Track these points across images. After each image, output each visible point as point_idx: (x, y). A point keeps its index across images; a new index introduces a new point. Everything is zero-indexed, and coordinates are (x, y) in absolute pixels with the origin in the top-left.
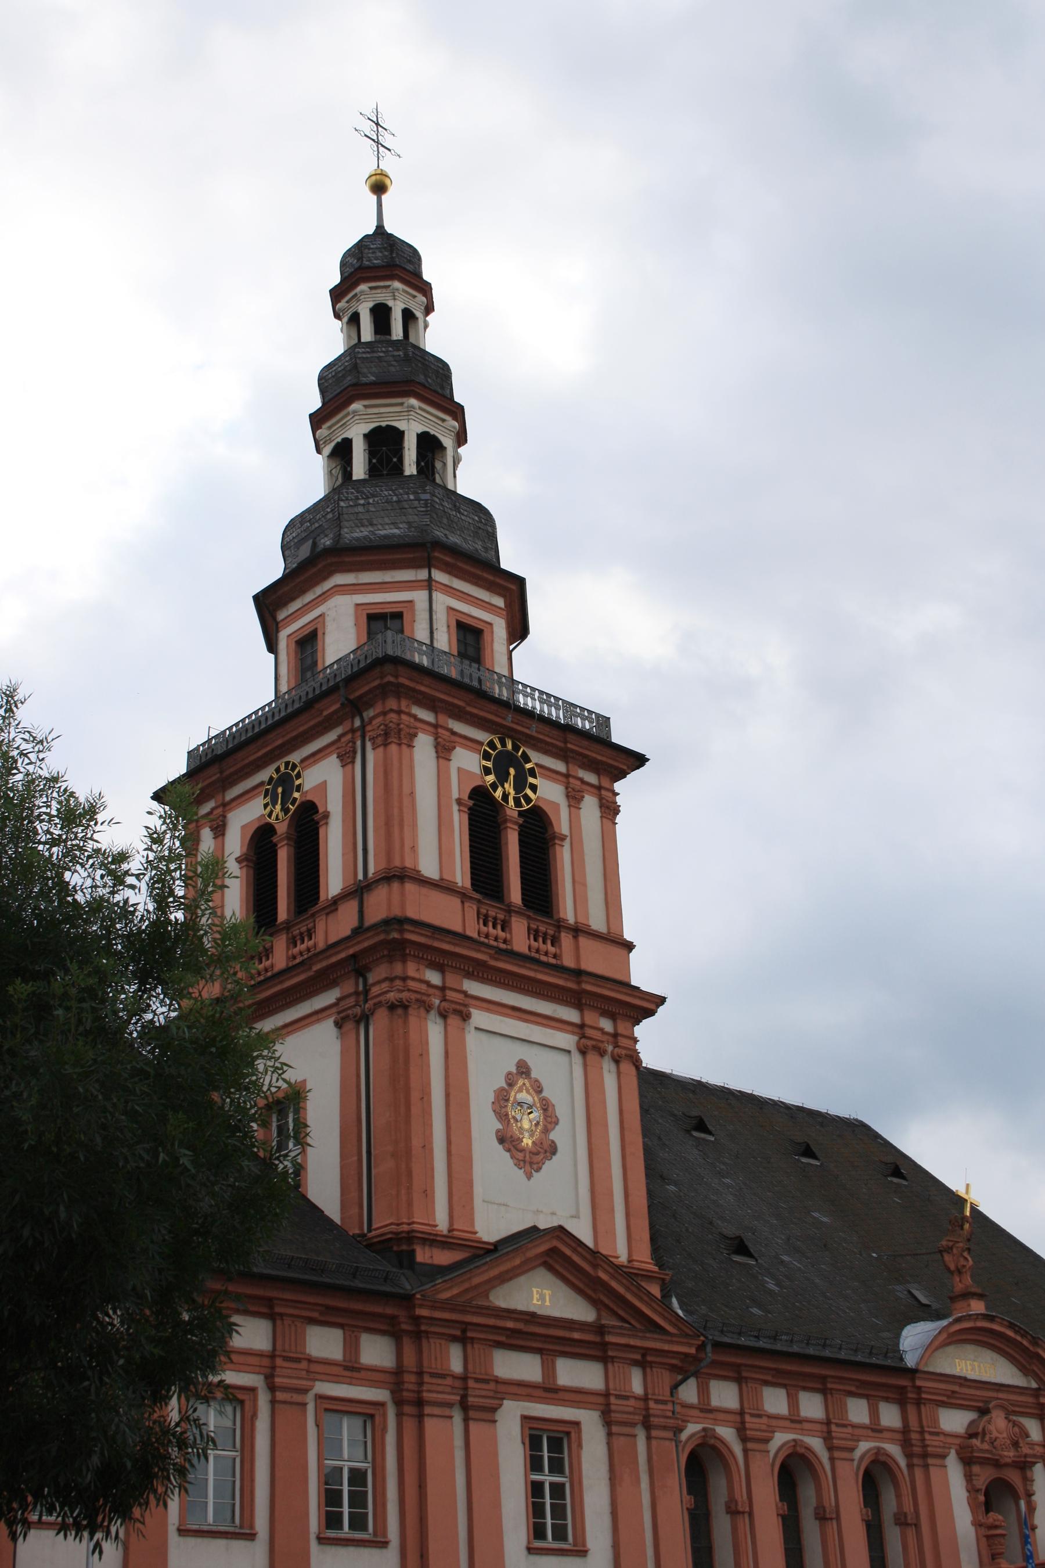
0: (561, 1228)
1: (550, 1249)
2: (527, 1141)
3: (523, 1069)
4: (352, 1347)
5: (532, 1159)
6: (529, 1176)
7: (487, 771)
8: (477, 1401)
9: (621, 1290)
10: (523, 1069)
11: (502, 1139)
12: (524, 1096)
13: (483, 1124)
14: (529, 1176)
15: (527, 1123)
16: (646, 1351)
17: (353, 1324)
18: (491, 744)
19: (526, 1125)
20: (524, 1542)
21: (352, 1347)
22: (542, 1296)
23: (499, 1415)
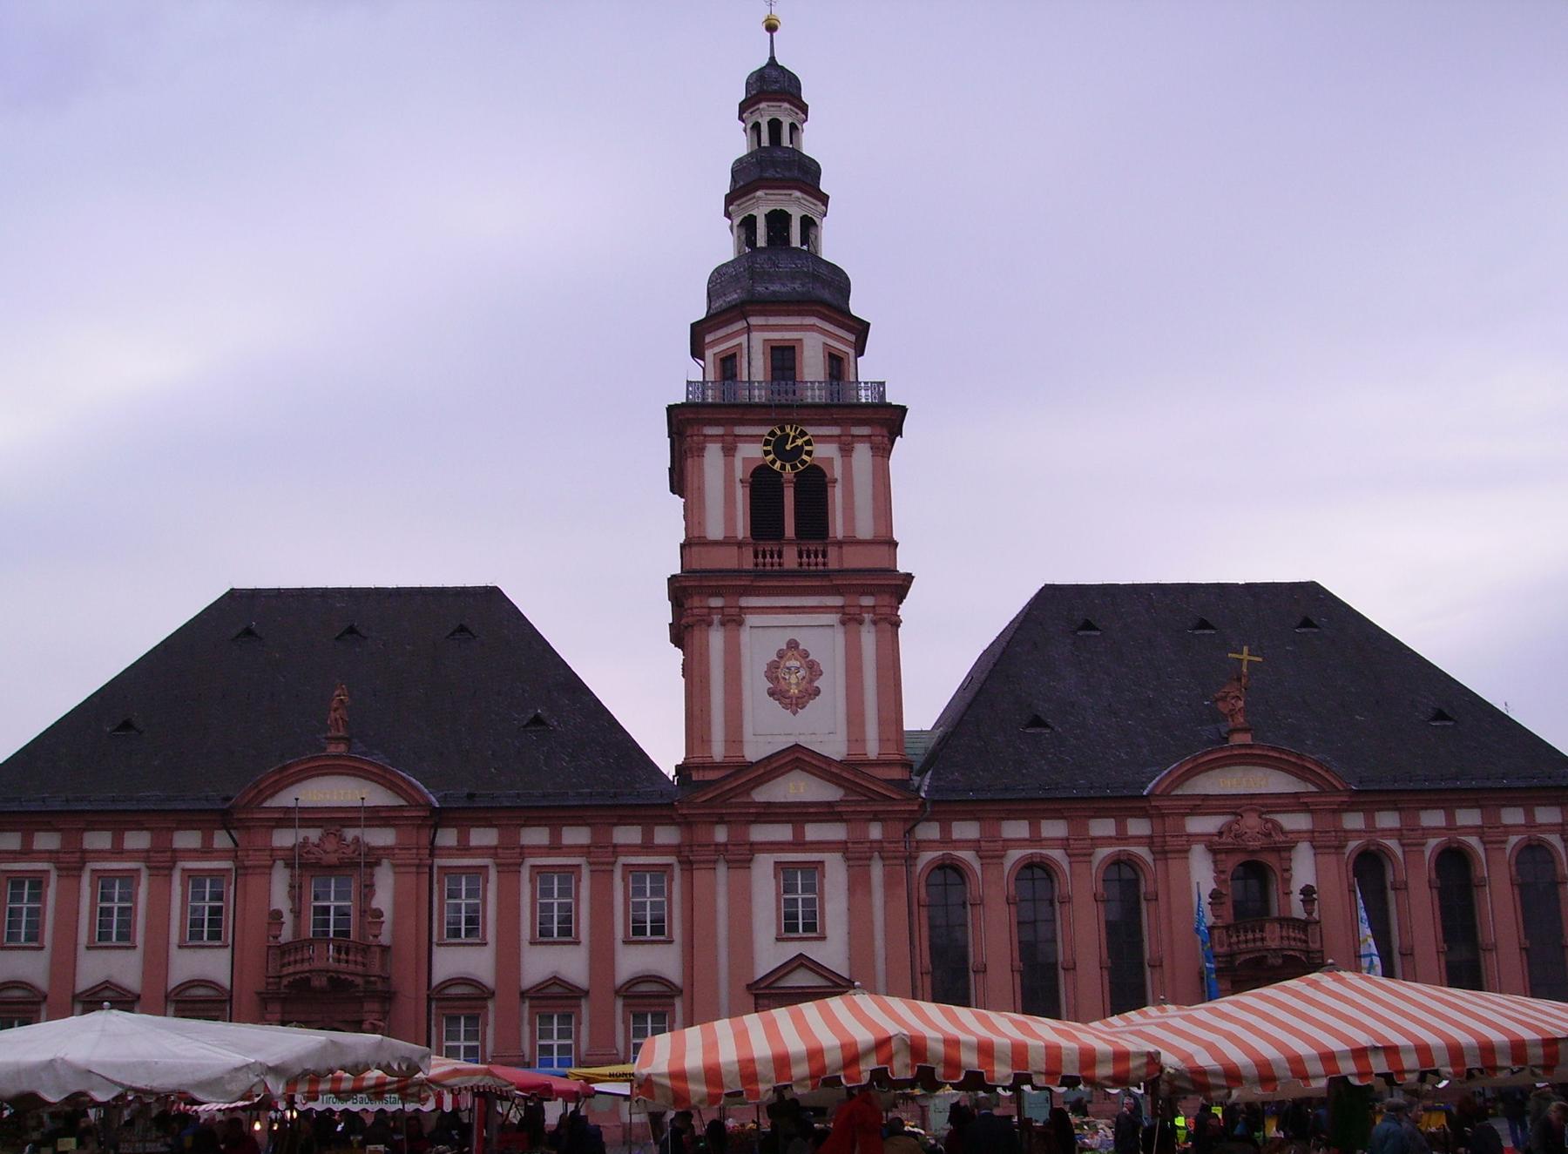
0: (797, 745)
1: (797, 758)
2: (794, 691)
3: (793, 645)
4: (1121, 827)
5: (795, 703)
6: (795, 713)
7: (767, 453)
8: (741, 857)
9: (851, 777)
10: (793, 645)
11: (772, 693)
12: (794, 663)
13: (755, 684)
14: (795, 713)
15: (793, 683)
16: (876, 813)
17: (1369, 810)
18: (772, 434)
19: (793, 680)
20: (773, 932)
21: (1121, 827)
22: (797, 788)
23: (754, 865)
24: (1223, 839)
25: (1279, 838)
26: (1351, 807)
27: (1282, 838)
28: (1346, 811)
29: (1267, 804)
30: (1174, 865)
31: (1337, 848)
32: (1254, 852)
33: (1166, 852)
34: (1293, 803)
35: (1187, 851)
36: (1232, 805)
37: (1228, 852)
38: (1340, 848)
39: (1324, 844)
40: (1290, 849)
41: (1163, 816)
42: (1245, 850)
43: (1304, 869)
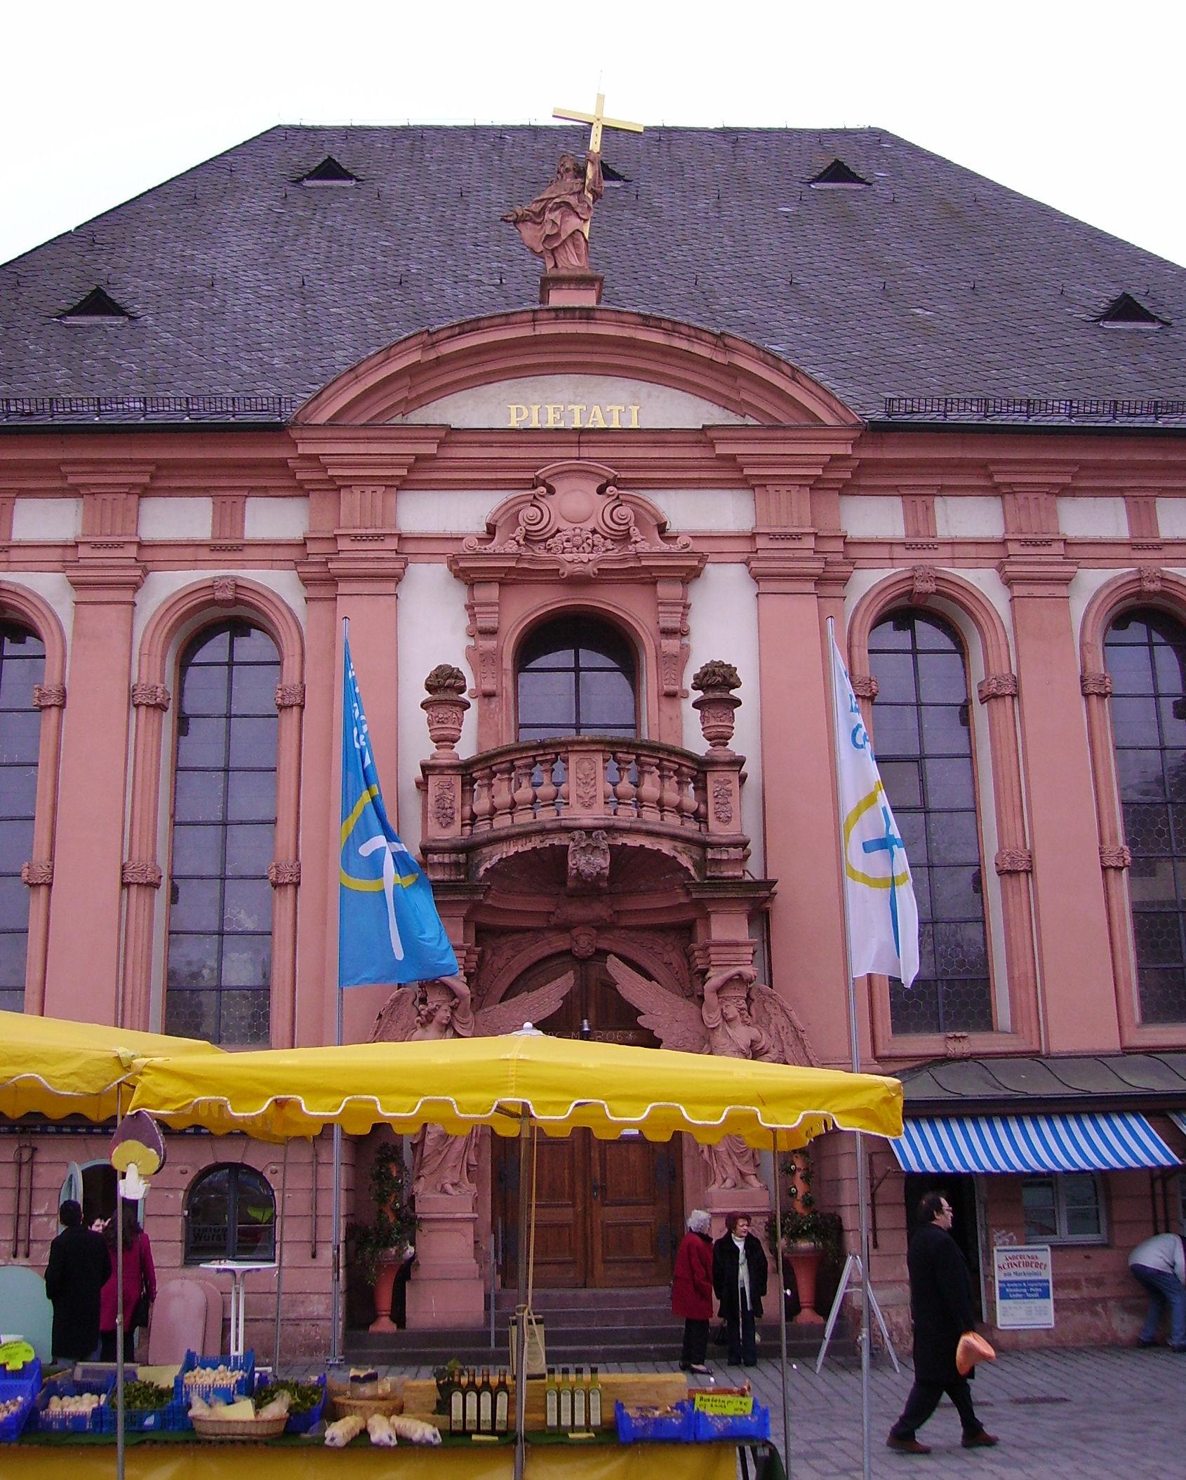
17: (918, 486)
24: (492, 547)
25: (647, 544)
26: (857, 480)
27: (665, 547)
28: (848, 489)
29: (625, 465)
30: (356, 609)
31: (820, 581)
32: (578, 581)
33: (332, 580)
34: (706, 461)
35: (397, 578)
36: (524, 464)
37: (511, 578)
38: (828, 581)
39: (797, 570)
40: (690, 575)
41: (336, 487)
42: (552, 577)
43: (724, 622)
